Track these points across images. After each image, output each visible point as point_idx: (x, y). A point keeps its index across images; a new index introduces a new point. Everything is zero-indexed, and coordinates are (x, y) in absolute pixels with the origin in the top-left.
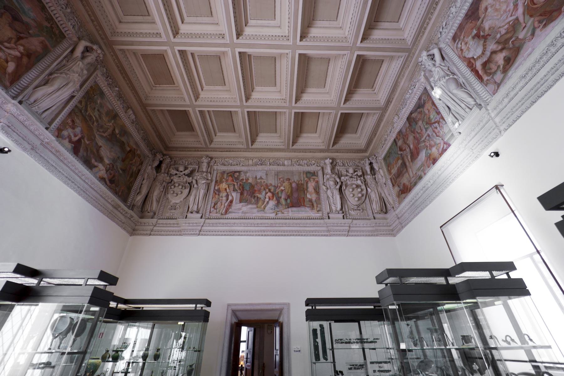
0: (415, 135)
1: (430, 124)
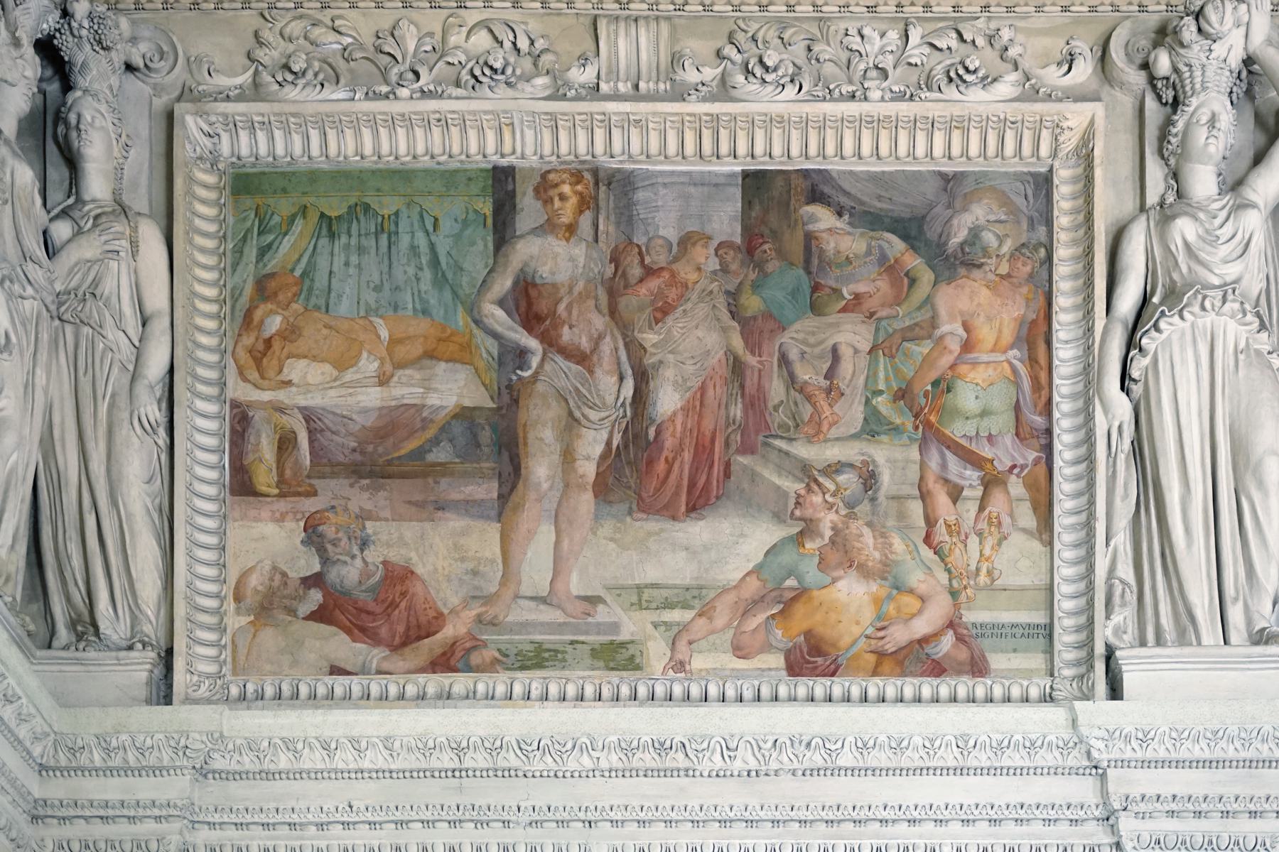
0: (752, 360)
1: (928, 425)
